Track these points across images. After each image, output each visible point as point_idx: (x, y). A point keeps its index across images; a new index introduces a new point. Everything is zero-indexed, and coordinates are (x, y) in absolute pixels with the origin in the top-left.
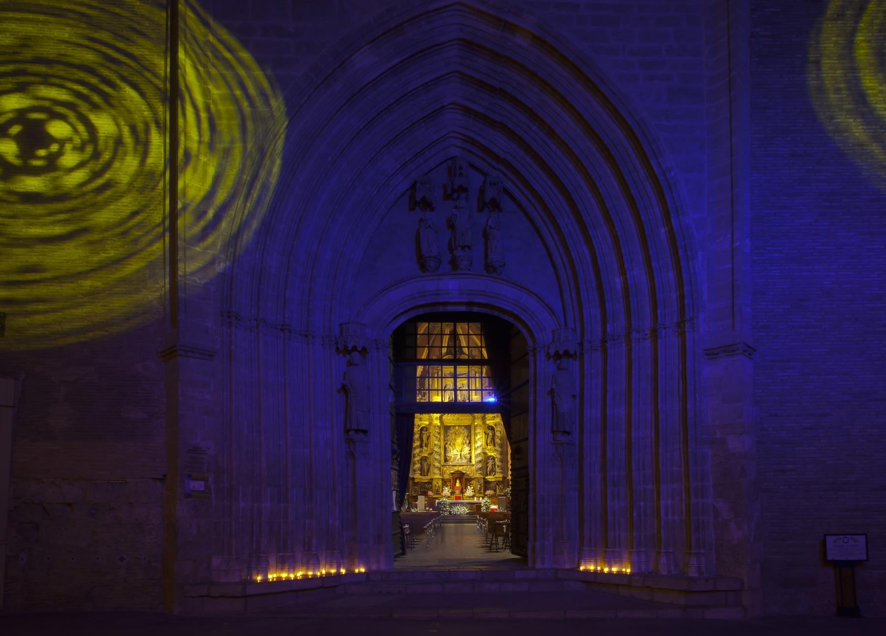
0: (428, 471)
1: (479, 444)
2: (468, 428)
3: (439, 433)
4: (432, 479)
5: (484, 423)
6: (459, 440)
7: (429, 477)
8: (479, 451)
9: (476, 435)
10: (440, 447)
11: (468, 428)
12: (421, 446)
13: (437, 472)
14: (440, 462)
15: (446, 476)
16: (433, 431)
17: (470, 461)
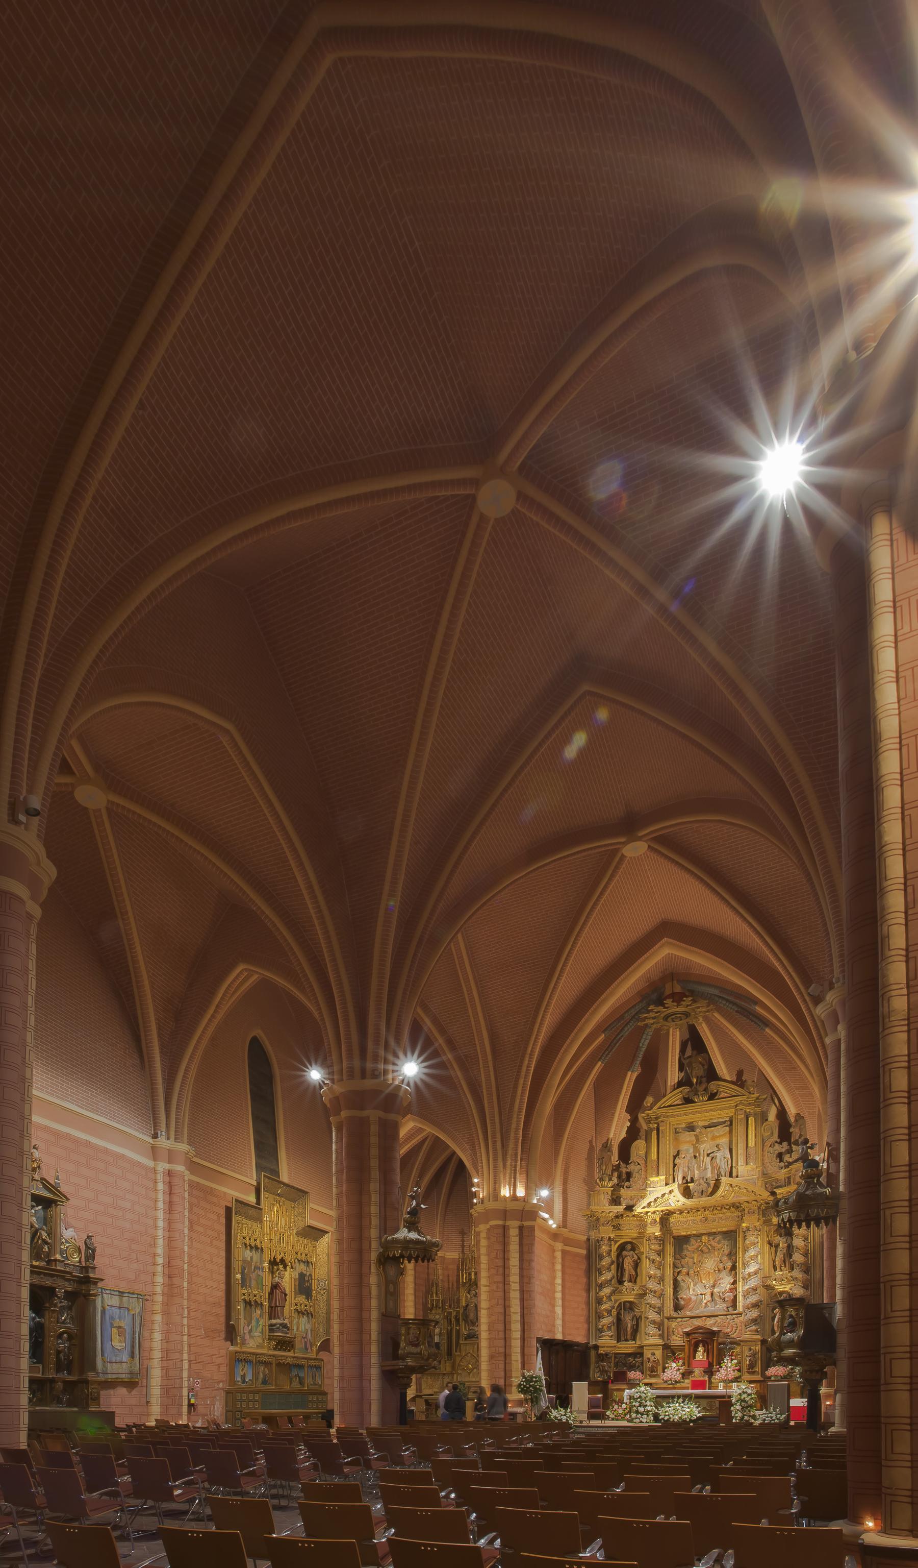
0: (636, 1330)
1: (752, 1269)
3: (661, 1253)
4: (642, 1347)
6: (710, 1264)
7: (638, 1343)
8: (753, 1282)
10: (661, 1280)
12: (621, 1282)
13: (652, 1330)
14: (660, 1311)
15: (677, 1340)
16: (648, 1250)
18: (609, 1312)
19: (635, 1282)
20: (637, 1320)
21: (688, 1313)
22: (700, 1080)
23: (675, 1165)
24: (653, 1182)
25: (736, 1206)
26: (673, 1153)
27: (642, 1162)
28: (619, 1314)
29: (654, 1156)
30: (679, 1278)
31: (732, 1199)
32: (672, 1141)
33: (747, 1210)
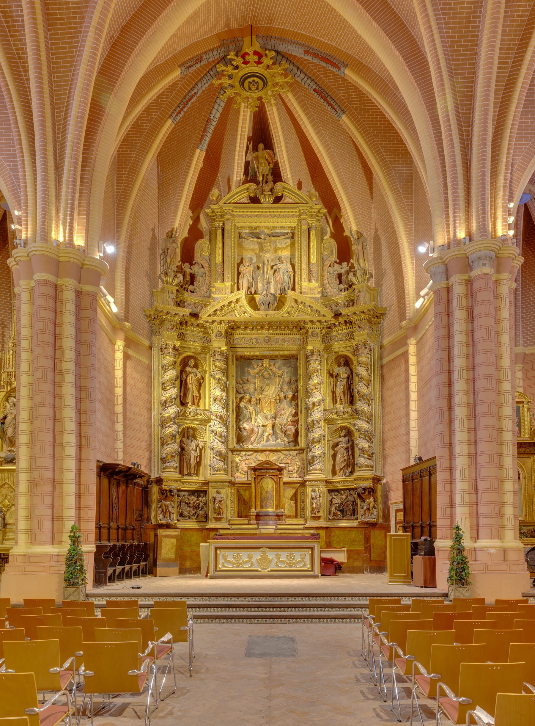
3: (225, 372)
4: (207, 483)
5: (328, 349)
9: (308, 376)
12: (183, 404)
17: (296, 441)
18: (173, 437)
19: (198, 405)
20: (201, 450)
21: (250, 447)
22: (264, 181)
23: (239, 273)
24: (217, 289)
25: (300, 327)
26: (237, 261)
27: (206, 265)
28: (181, 441)
29: (219, 259)
30: (242, 405)
32: (236, 245)
33: (310, 331)
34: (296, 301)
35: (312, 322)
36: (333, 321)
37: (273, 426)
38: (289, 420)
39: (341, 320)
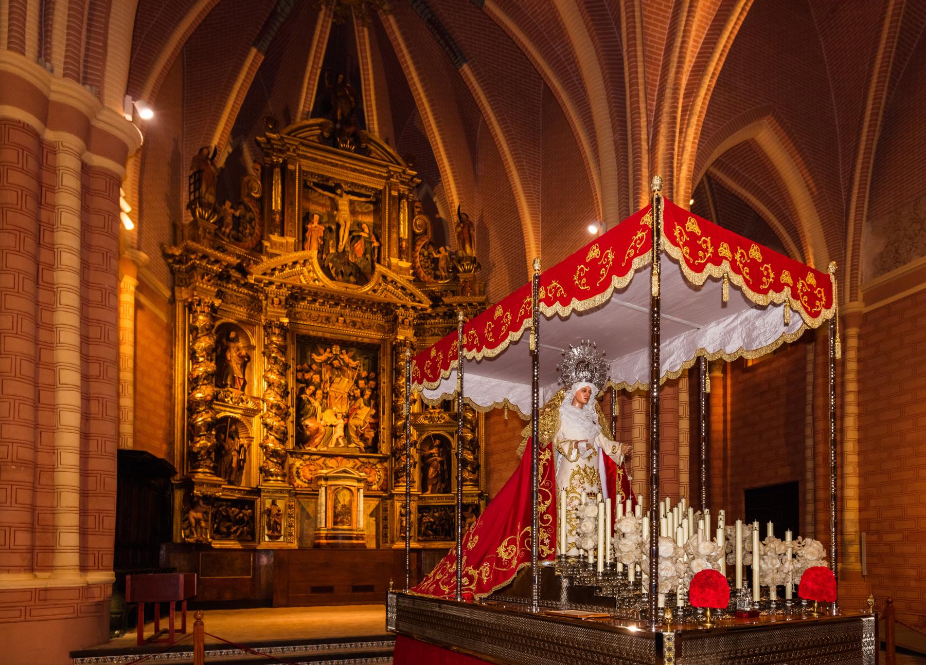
2: (370, 353)
11: (370, 353)
25: (387, 309)
31: (380, 297)
33: (400, 318)
34: (384, 277)
35: (404, 306)
36: (429, 311)
37: (346, 427)
38: (368, 421)
39: (441, 310)
